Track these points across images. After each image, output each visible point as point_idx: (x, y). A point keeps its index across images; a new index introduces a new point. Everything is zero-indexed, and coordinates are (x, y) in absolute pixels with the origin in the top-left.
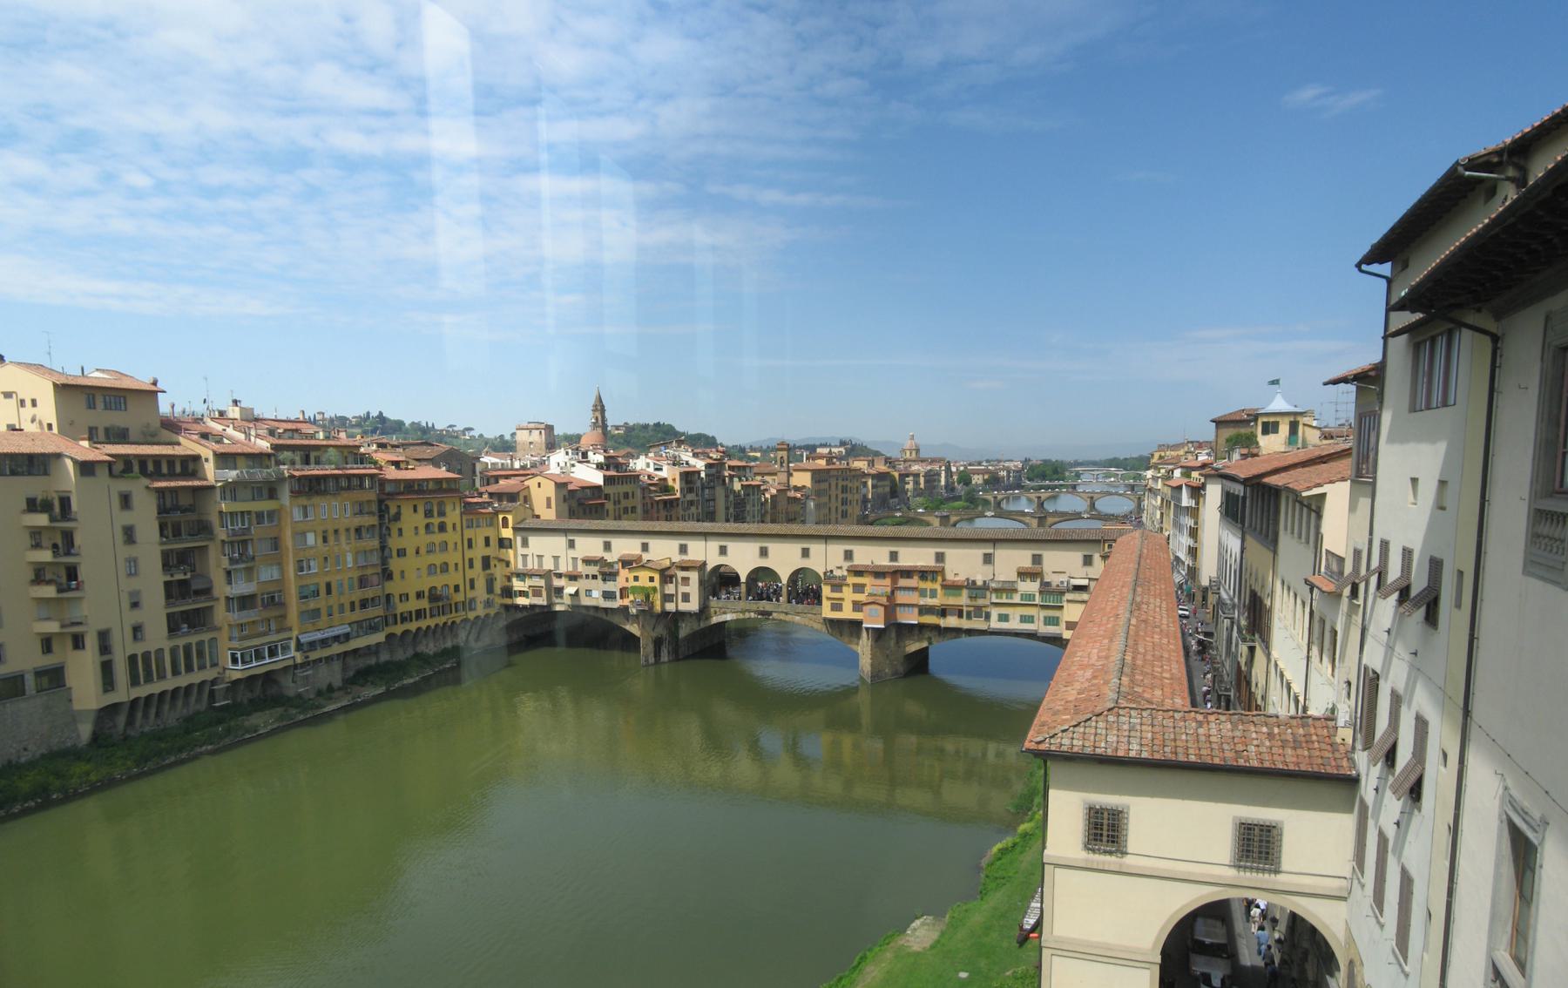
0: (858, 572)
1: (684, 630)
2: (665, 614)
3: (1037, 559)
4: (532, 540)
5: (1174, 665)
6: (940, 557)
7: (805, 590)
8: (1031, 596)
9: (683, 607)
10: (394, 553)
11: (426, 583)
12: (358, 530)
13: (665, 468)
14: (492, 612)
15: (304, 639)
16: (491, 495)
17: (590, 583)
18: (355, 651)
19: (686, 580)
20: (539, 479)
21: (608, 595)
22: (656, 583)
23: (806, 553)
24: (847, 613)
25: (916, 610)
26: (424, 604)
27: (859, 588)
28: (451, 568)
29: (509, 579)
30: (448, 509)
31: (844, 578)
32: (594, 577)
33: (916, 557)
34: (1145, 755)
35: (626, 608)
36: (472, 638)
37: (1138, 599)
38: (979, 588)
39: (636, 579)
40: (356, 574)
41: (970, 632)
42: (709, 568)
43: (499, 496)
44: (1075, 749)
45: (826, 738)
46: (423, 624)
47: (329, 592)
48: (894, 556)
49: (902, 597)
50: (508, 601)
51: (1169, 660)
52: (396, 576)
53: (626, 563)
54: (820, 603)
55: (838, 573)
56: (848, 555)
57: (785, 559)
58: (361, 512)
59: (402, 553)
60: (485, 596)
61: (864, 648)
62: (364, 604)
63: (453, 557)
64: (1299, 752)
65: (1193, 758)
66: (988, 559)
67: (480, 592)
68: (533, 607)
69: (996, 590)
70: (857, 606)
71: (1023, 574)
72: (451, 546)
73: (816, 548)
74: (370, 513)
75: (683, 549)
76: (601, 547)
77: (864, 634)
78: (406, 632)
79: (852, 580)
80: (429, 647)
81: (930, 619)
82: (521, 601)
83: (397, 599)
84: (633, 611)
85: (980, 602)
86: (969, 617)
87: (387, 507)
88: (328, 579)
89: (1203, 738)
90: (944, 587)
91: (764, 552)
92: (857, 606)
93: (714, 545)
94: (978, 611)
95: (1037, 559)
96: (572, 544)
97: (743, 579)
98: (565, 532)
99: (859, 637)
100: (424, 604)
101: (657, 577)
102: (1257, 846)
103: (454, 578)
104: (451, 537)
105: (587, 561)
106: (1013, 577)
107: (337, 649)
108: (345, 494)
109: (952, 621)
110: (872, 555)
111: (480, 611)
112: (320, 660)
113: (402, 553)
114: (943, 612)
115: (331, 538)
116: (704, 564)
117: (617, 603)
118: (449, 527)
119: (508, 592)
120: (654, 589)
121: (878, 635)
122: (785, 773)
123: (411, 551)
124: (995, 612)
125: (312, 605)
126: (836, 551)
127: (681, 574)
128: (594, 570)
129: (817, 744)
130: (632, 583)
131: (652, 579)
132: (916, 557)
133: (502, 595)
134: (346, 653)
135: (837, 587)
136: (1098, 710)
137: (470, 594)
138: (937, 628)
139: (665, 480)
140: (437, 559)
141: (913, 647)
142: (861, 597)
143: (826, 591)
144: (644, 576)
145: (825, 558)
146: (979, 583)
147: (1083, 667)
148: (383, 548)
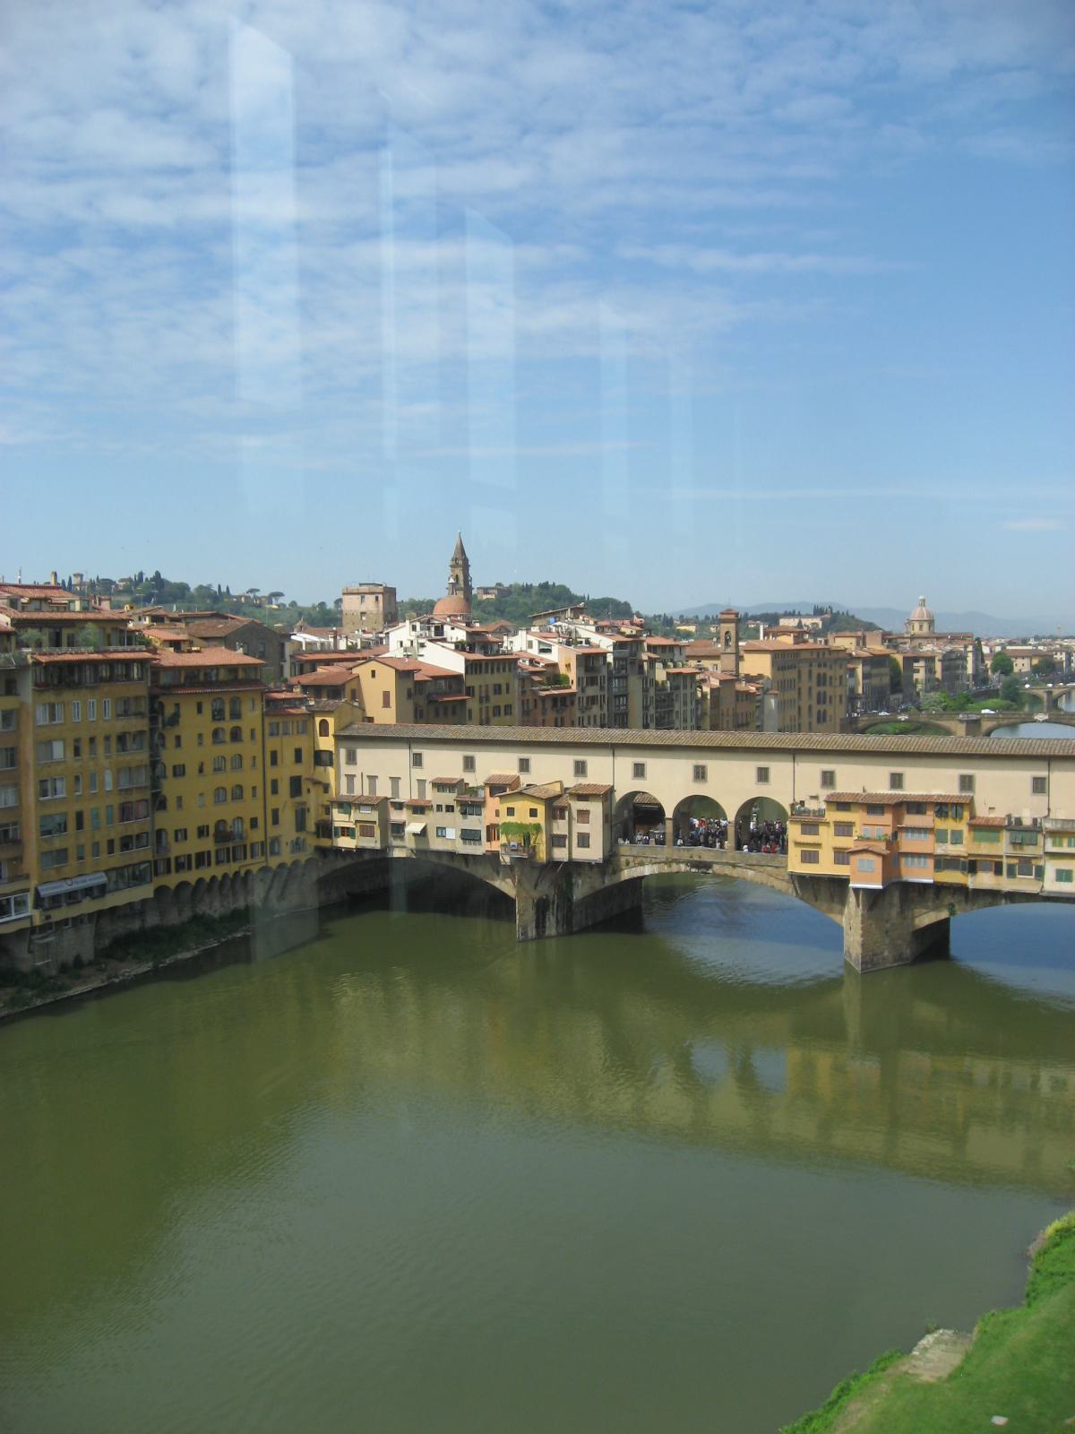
0: (843, 805)
1: (581, 890)
2: (553, 864)
4: (363, 754)
6: (967, 783)
7: (763, 830)
9: (580, 854)
10: (169, 772)
11: (212, 815)
12: (121, 739)
13: (555, 648)
14: (303, 857)
15: (46, 891)
16: (305, 688)
18: (113, 910)
19: (584, 815)
20: (373, 665)
21: (469, 836)
22: (541, 819)
23: (763, 775)
24: (826, 866)
25: (930, 863)
26: (208, 844)
27: (844, 829)
28: (247, 793)
29: (328, 811)
30: (246, 708)
31: (821, 813)
32: (450, 809)
35: (495, 855)
36: (274, 894)
38: (1027, 830)
39: (511, 811)
40: (116, 801)
41: (1013, 897)
42: (618, 795)
43: (316, 690)
45: (793, 1056)
47: (80, 825)
48: (896, 781)
49: (908, 843)
50: (325, 842)
52: (171, 803)
53: (496, 788)
54: (784, 850)
55: (811, 805)
56: (828, 779)
57: (732, 784)
58: (126, 714)
59: (179, 771)
61: (851, 918)
62: (126, 843)
63: (250, 778)
66: (1040, 786)
67: (287, 830)
68: (360, 851)
69: (1054, 834)
70: (842, 856)
72: (247, 762)
74: (139, 714)
75: (580, 768)
77: (852, 898)
78: (183, 885)
79: (834, 816)
80: (214, 907)
82: (345, 842)
84: (506, 859)
85: (1029, 851)
86: (1011, 873)
87: (162, 706)
88: (78, 807)
90: (974, 827)
91: (700, 774)
92: (842, 856)
93: (625, 762)
94: (1026, 866)
96: (417, 761)
97: (669, 813)
98: (409, 742)
99: (843, 902)
100: (208, 844)
101: (541, 809)
103: (251, 807)
104: (248, 748)
105: (440, 786)
107: (88, 906)
108: (106, 688)
109: (985, 880)
110: (868, 779)
111: (286, 856)
112: (65, 922)
113: (179, 771)
114: (972, 866)
115: (85, 748)
116: (611, 790)
118: (246, 734)
119: (326, 829)
120: (537, 827)
121: (872, 900)
122: (728, 1105)
123: (191, 770)
124: (1051, 868)
125: (58, 843)
126: (810, 771)
127: (577, 805)
128: (448, 798)
129: (780, 1064)
130: (504, 819)
131: (533, 813)
134: (100, 913)
135: (811, 826)
137: (273, 832)
138: (961, 890)
139: (555, 665)
140: (228, 780)
141: (926, 918)
142: (847, 842)
143: (794, 832)
144: (523, 806)
145: (793, 783)
146: (1027, 822)
148: (154, 763)
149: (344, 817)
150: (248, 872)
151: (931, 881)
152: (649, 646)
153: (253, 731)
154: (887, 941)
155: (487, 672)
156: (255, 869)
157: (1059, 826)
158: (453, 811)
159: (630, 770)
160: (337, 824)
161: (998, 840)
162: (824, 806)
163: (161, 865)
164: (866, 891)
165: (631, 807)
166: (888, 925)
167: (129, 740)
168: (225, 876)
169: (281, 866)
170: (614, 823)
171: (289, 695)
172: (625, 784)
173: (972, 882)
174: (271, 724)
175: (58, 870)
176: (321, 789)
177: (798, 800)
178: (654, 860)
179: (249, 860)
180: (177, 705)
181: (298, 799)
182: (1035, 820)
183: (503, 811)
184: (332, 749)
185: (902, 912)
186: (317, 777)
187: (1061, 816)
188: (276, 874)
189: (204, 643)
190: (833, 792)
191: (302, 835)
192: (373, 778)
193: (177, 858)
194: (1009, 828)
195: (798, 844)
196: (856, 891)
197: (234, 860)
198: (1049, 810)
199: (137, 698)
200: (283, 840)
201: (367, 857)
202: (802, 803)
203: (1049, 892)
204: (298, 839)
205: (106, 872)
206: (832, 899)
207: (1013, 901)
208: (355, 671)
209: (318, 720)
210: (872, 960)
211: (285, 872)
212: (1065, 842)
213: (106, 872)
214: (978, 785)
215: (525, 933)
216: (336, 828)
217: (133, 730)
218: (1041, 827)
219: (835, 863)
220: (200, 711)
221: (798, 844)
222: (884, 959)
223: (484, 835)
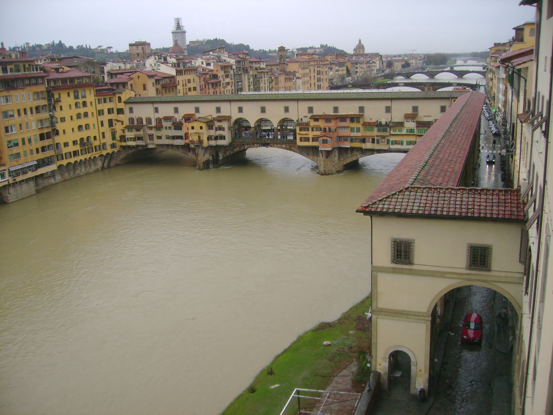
2: (211, 147)
3: (415, 109)
4: (136, 107)
5: (458, 165)
6: (361, 109)
8: (412, 130)
9: (221, 142)
10: (59, 120)
11: (78, 136)
12: (37, 108)
13: (212, 64)
14: (116, 150)
16: (112, 84)
18: (42, 175)
20: (138, 74)
23: (287, 110)
26: (78, 148)
28: (91, 127)
29: (124, 131)
32: (170, 128)
34: (420, 212)
35: (188, 145)
37: (452, 130)
38: (384, 126)
39: (193, 128)
43: (117, 84)
44: (385, 210)
46: (78, 159)
47: (24, 143)
48: (336, 109)
50: (124, 144)
51: (456, 162)
52: (61, 132)
53: (188, 118)
55: (305, 120)
56: (311, 110)
57: (275, 114)
58: (38, 99)
59: (63, 120)
62: (43, 149)
63: (91, 120)
64: (500, 208)
65: (445, 213)
66: (388, 110)
67: (108, 140)
68: (137, 146)
71: (407, 117)
72: (90, 115)
73: (292, 106)
74: (43, 98)
75: (218, 110)
76: (173, 110)
78: (69, 164)
79: (313, 123)
81: (357, 145)
83: (62, 145)
84: (192, 146)
86: (378, 142)
87: (53, 95)
88: (22, 136)
89: (452, 202)
91: (263, 110)
93: (235, 106)
95: (415, 109)
96: (156, 110)
98: (153, 103)
99: (318, 156)
100: (78, 148)
101: (204, 126)
102: (479, 257)
103: (92, 133)
104: (90, 109)
105: (167, 119)
107: (31, 174)
108: (28, 88)
109: (368, 145)
111: (109, 150)
112: (23, 181)
113: (63, 120)
118: (88, 104)
121: (328, 154)
123: (68, 119)
125: (15, 150)
126: (304, 106)
127: (217, 124)
128: (169, 124)
130: (191, 131)
131: (201, 128)
132: (348, 109)
133: (121, 141)
134: (36, 177)
136: (401, 189)
137: (103, 141)
139: (212, 71)
140: (83, 122)
142: (318, 133)
144: (197, 125)
146: (384, 123)
148: (52, 117)
149: (130, 133)
150: (95, 157)
152: (250, 62)
153: (91, 102)
156: (97, 156)
159: (237, 110)
161: (373, 130)
162: (309, 120)
163: (60, 157)
164: (325, 151)
167: (41, 109)
168: (85, 159)
169: (108, 154)
171: (105, 88)
172: (235, 115)
173: (365, 146)
174: (99, 100)
175: (17, 161)
176: (120, 123)
177: (300, 118)
179: (94, 153)
180: (59, 94)
181: (112, 128)
182: (386, 123)
185: (339, 158)
187: (396, 120)
189: (69, 69)
191: (115, 142)
193: (65, 154)
194: (377, 126)
195: (299, 134)
196: (321, 151)
197: (89, 153)
199: (42, 92)
201: (140, 148)
202: (301, 119)
205: (37, 161)
206: (314, 154)
207: (379, 153)
208: (131, 77)
209: (117, 96)
211: (109, 156)
212: (397, 131)
213: (37, 161)
214: (366, 110)
216: (128, 138)
217: (41, 105)
220: (69, 96)
221: (299, 134)
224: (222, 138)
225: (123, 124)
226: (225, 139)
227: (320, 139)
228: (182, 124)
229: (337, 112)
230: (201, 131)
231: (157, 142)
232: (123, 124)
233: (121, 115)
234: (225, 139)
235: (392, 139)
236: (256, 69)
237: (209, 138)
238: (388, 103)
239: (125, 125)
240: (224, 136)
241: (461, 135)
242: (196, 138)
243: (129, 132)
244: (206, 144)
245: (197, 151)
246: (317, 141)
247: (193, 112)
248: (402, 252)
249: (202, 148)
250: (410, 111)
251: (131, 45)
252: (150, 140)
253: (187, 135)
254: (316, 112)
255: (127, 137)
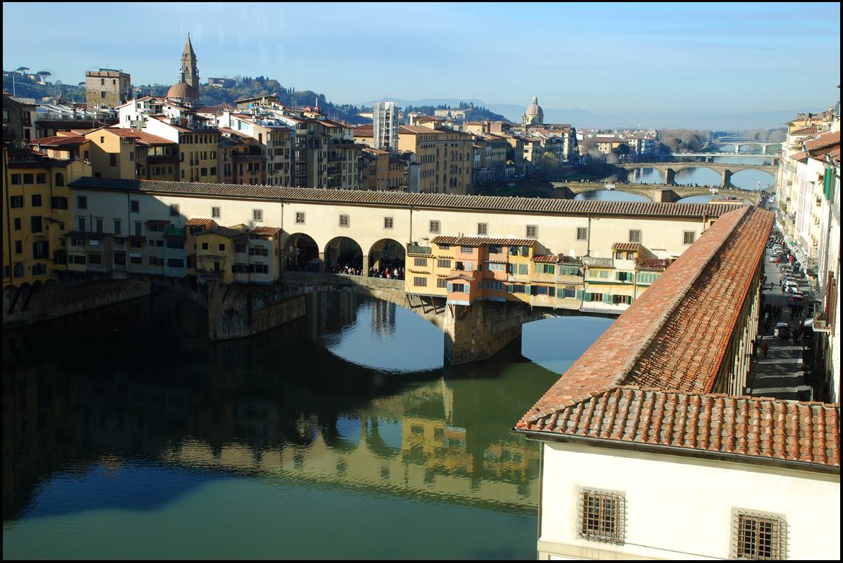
2: (238, 285)
3: (634, 235)
4: (93, 198)
6: (531, 230)
14: (43, 278)
17: (159, 252)
20: (103, 132)
21: (174, 263)
23: (388, 223)
24: (432, 289)
27: (444, 263)
29: (63, 243)
32: (160, 244)
33: (507, 226)
36: (17, 307)
45: (407, 423)
48: (482, 228)
50: (61, 267)
54: (402, 277)
55: (422, 244)
56: (434, 226)
60: (35, 262)
66: (582, 234)
68: (89, 274)
71: (619, 250)
79: (437, 251)
82: (73, 267)
89: (702, 424)
91: (344, 221)
92: (442, 283)
93: (292, 209)
94: (569, 293)
95: (634, 235)
101: (227, 243)
106: (609, 254)
109: (542, 300)
110: (460, 224)
111: (29, 278)
116: (281, 231)
117: (183, 272)
119: (61, 257)
120: (224, 258)
121: (460, 312)
128: (158, 235)
131: (222, 247)
133: (55, 261)
143: (409, 262)
145: (410, 226)
147: (610, 348)
149: (75, 248)
151: (504, 300)
154: (473, 342)
155: (196, 142)
157: (594, 263)
158: (162, 245)
160: (69, 254)
164: (459, 308)
165: (296, 244)
166: (474, 331)
169: (25, 285)
170: (282, 255)
172: (291, 228)
177: (413, 241)
178: (310, 283)
181: (38, 234)
183: (200, 246)
184: (67, 196)
185: (484, 322)
186: (54, 217)
187: (595, 254)
188: (19, 290)
190: (438, 235)
191: (42, 261)
192: (100, 223)
198: (589, 251)
200: (26, 265)
201: (96, 278)
202: (416, 243)
203: (586, 309)
204: (39, 264)
210: (462, 355)
212: (599, 274)
215: (215, 336)
216: (71, 257)
218: (581, 263)
219: (438, 286)
222: (471, 354)
223: (185, 262)
224: (263, 269)
225: (62, 227)
226: (266, 272)
227: (450, 283)
228: (185, 237)
229: (485, 232)
230: (220, 253)
231: (131, 268)
232: (62, 227)
233: (61, 212)
234: (266, 272)
235: (590, 289)
236: (336, 141)
237: (237, 268)
238: (582, 222)
239: (66, 230)
240: (266, 267)
241: (723, 290)
242: (209, 266)
243: (74, 244)
244: (229, 277)
245: (210, 290)
246: (444, 286)
247: (207, 216)
248: (600, 515)
249: (222, 285)
250: (625, 239)
251: (90, 75)
252: (116, 262)
253: (192, 261)
254: (445, 232)
255: (69, 254)
